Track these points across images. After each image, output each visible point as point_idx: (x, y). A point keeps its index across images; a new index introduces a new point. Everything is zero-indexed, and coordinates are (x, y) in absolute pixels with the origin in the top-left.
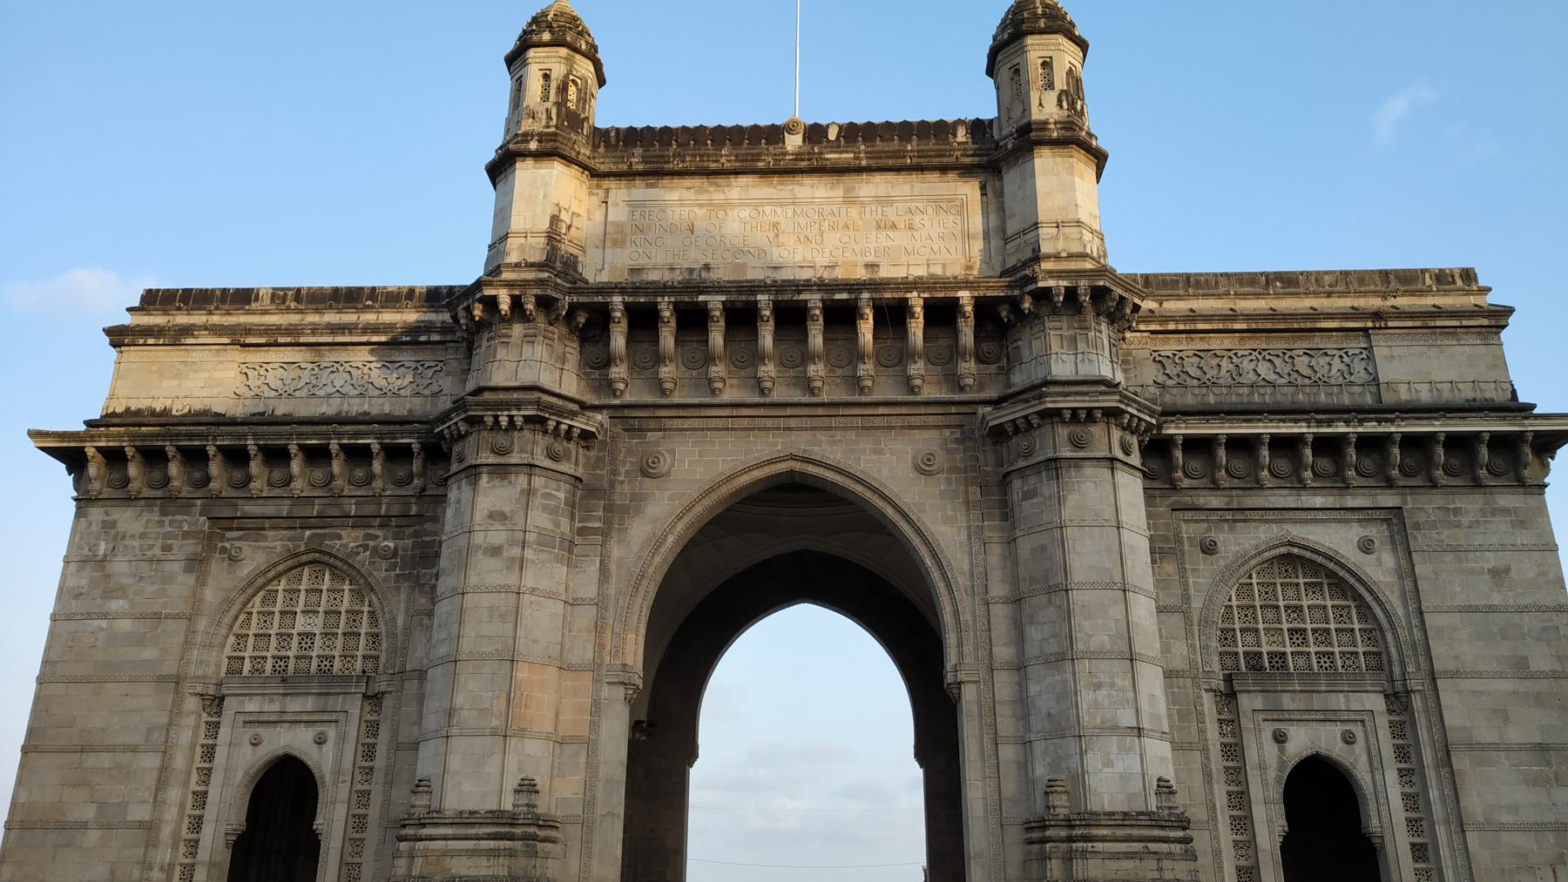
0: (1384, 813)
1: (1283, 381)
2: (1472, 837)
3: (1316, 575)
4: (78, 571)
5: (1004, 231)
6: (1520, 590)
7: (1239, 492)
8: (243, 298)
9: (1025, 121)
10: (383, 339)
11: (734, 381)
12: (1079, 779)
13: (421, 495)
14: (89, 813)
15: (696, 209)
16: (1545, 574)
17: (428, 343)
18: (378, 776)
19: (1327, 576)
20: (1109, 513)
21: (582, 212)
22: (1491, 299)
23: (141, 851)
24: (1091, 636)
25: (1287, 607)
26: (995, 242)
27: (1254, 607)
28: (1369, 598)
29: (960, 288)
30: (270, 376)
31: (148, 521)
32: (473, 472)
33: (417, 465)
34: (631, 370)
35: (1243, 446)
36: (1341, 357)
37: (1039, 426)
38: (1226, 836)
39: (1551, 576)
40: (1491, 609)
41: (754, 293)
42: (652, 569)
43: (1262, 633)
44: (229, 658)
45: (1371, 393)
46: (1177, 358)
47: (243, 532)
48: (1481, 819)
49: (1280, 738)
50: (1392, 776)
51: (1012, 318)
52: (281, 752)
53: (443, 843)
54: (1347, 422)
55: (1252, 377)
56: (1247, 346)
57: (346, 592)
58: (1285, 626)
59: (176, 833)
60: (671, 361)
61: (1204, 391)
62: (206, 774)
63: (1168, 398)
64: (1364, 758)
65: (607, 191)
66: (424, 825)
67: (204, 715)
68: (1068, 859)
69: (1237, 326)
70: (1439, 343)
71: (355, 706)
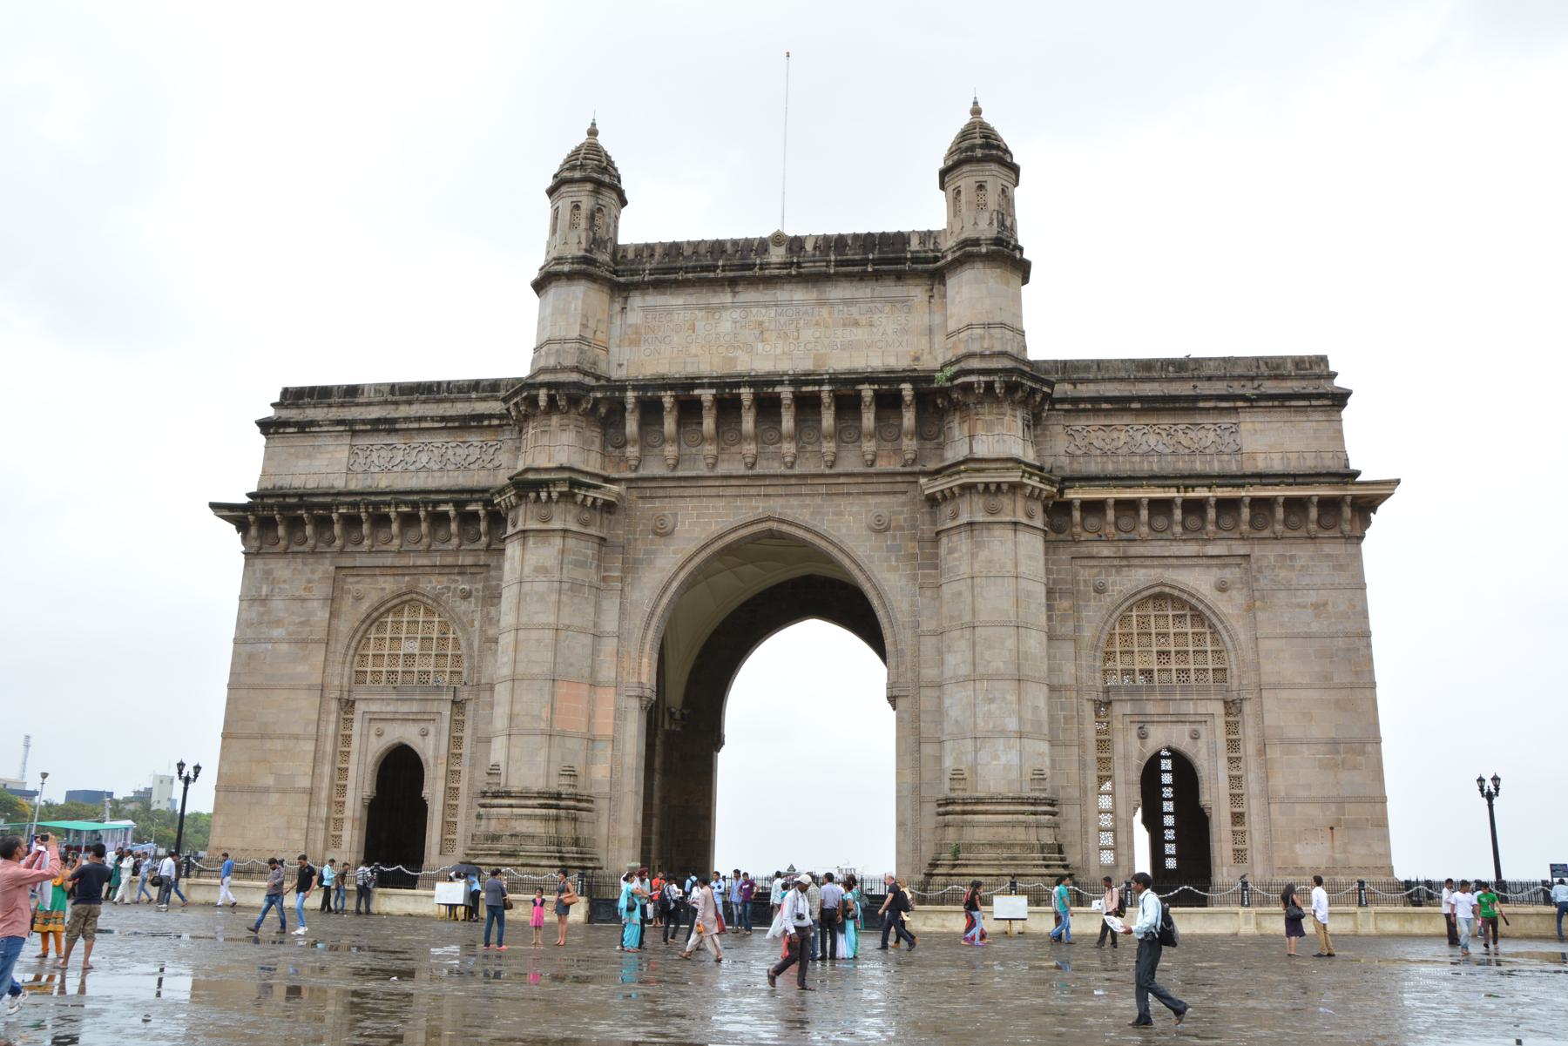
0: (1213, 790)
1: (1168, 451)
2: (1275, 808)
3: (1183, 608)
4: (250, 606)
5: (946, 327)
6: (1333, 620)
7: (1126, 543)
8: (352, 391)
9: (963, 236)
10: (457, 424)
11: (726, 457)
12: (974, 768)
13: (488, 549)
14: (270, 781)
15: (697, 312)
16: (1354, 606)
17: (490, 426)
18: (466, 760)
19: (1191, 609)
20: (1010, 566)
21: (605, 317)
22: (1339, 382)
23: (306, 809)
25: (1158, 634)
26: (939, 338)
27: (1132, 634)
28: (1220, 627)
29: (904, 380)
30: (375, 454)
31: (295, 569)
33: (483, 526)
34: (642, 449)
35: (1130, 506)
37: (961, 495)
39: (1358, 608)
40: (1309, 636)
41: (738, 385)
42: (660, 610)
43: (1136, 654)
44: (357, 672)
45: (1237, 461)
46: (1085, 433)
47: (359, 578)
48: (1283, 794)
49: (1143, 736)
50: (1223, 762)
51: (946, 404)
52: (396, 741)
53: (509, 810)
54: (1209, 487)
55: (1145, 448)
56: (1142, 422)
57: (436, 624)
58: (1155, 649)
59: (330, 797)
60: (673, 441)
61: (1105, 459)
63: (1075, 466)
64: (1204, 750)
65: (626, 298)
66: (496, 797)
67: (342, 713)
68: (961, 826)
69: (1135, 405)
70: (1293, 419)
71: (446, 710)
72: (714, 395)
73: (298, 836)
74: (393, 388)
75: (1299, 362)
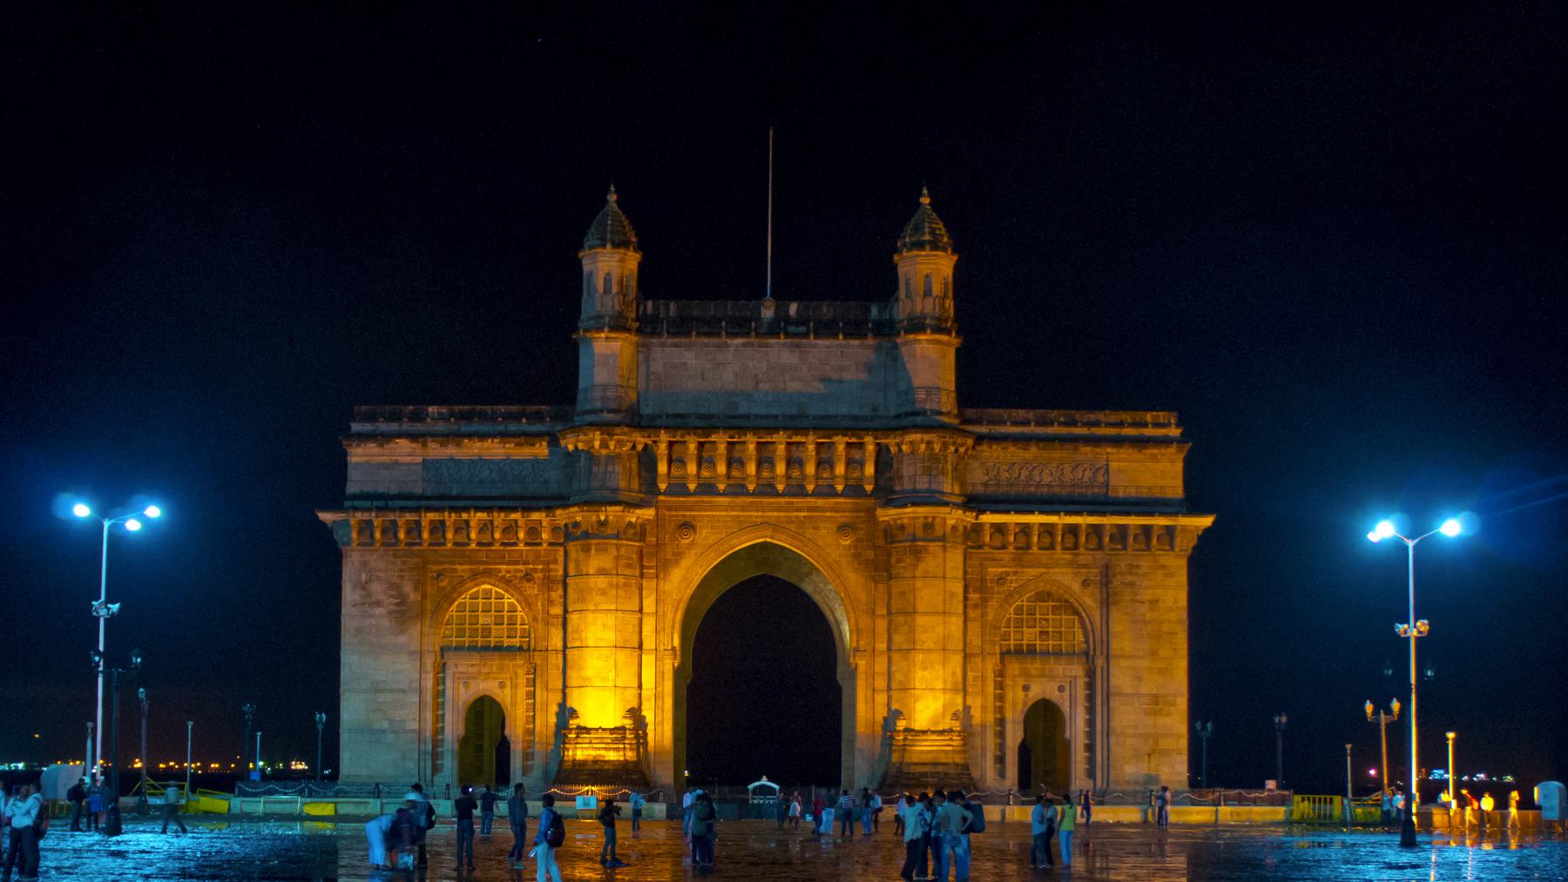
2: (1113, 740)
14: (385, 725)
24: (924, 642)
28: (1084, 614)
31: (388, 561)
36: (1091, 470)
38: (991, 742)
48: (1118, 732)
49: (1026, 688)
62: (439, 705)
64: (1068, 702)
73: (411, 765)
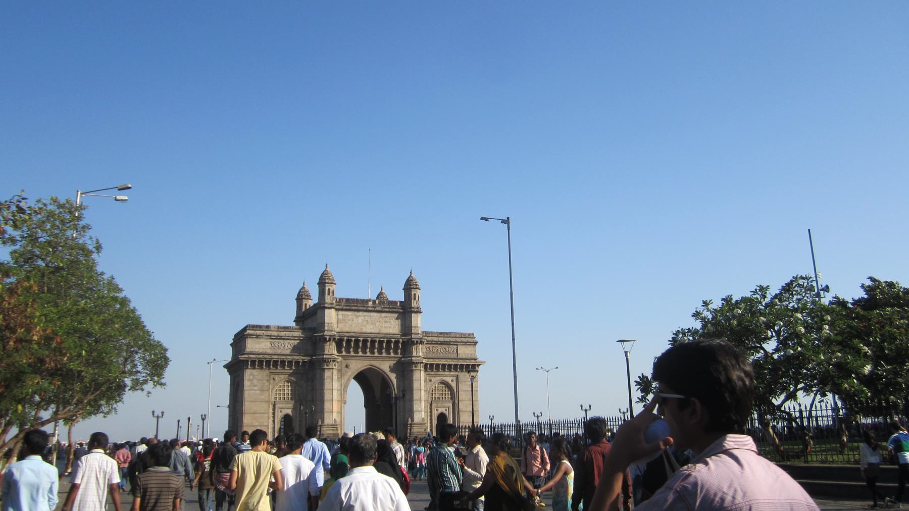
8: (268, 327)
22: (476, 339)
32: (324, 369)
33: (307, 365)
35: (438, 365)
41: (368, 338)
62: (274, 417)
69: (439, 343)
72: (363, 340)
74: (279, 327)
75: (469, 334)
